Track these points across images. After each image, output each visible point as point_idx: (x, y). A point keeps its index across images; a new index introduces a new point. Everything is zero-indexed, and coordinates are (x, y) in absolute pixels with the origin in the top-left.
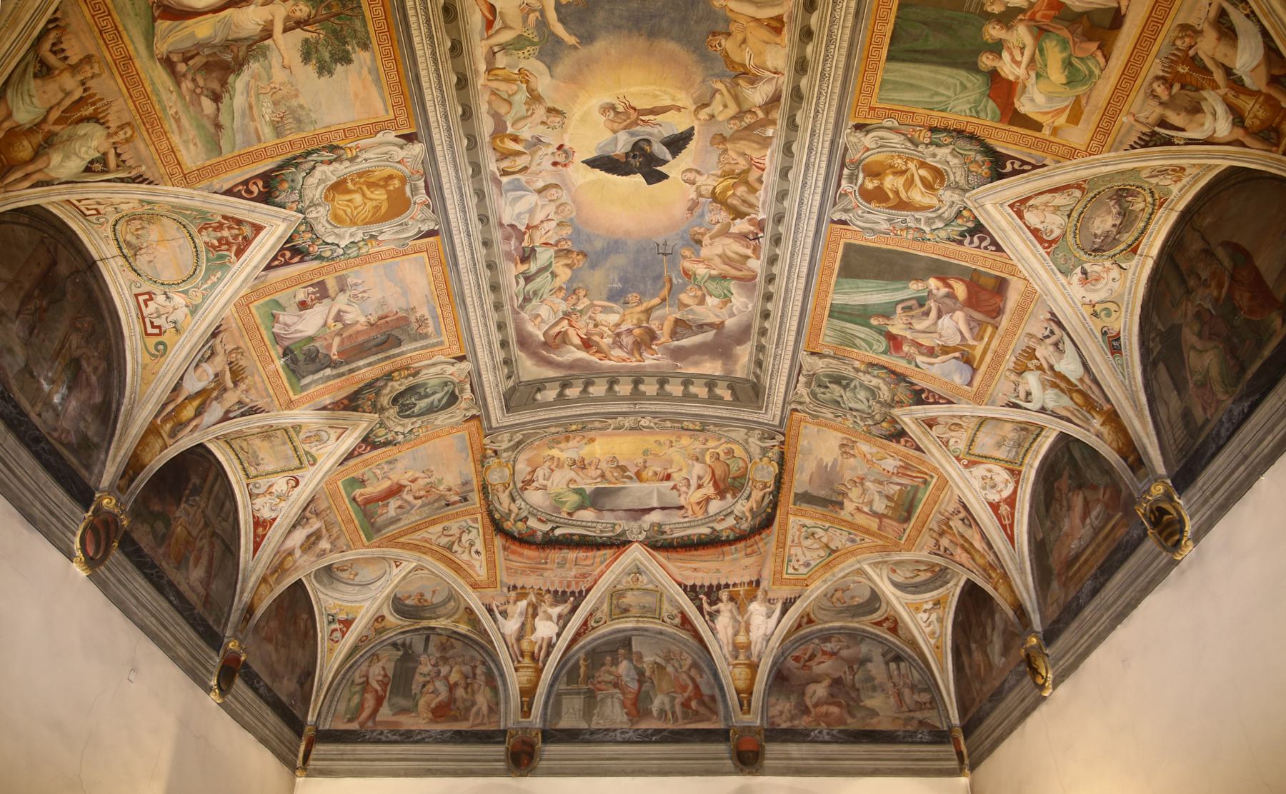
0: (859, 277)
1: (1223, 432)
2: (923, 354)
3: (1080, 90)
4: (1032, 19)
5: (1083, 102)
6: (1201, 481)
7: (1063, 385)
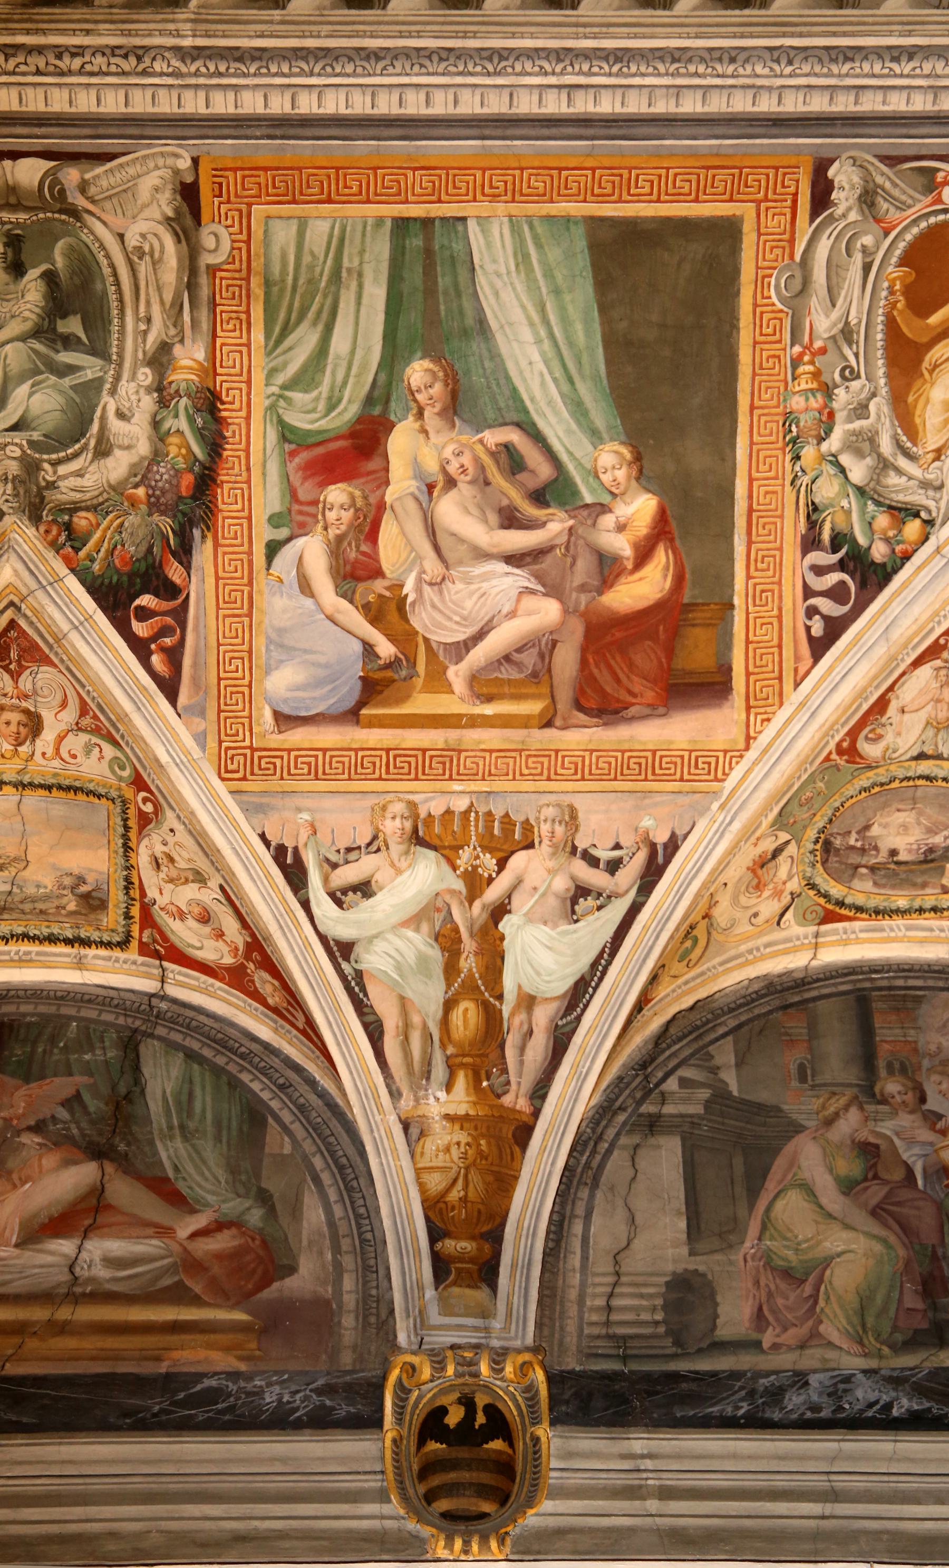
0: (603, 284)
1: (794, 1401)
2: (336, 549)
7: (469, 963)
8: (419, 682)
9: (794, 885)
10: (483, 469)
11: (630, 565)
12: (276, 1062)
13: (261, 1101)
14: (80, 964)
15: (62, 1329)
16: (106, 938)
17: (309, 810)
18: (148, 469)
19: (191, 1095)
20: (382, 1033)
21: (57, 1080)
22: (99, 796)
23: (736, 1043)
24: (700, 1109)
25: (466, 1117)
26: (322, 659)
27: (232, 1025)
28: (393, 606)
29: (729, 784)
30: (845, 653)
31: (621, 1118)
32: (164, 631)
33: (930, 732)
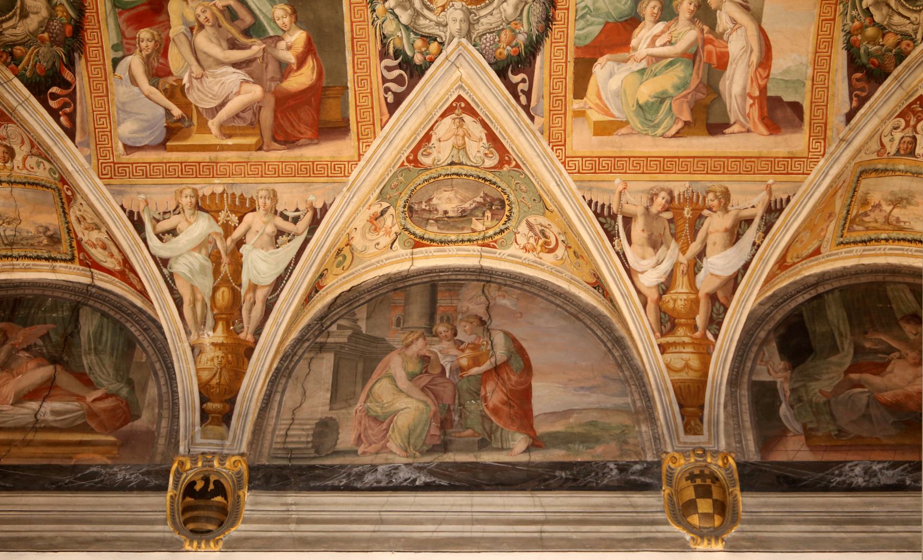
2: (147, 61)
3: (636, 123)
4: (705, 42)
5: (624, 131)
6: (291, 498)
8: (194, 128)
9: (396, 229)
10: (217, 19)
11: (295, 67)
12: (144, 318)
13: (134, 336)
14: (53, 270)
15: (28, 443)
16: (63, 257)
17: (144, 193)
18: (48, 23)
19: (101, 334)
20: (182, 303)
21: (39, 326)
22: (48, 188)
23: (368, 307)
24: (345, 340)
25: (222, 344)
26: (145, 118)
27: (125, 299)
28: (178, 90)
29: (351, 178)
30: (405, 111)
31: (307, 344)
32: (65, 105)
33: (455, 151)
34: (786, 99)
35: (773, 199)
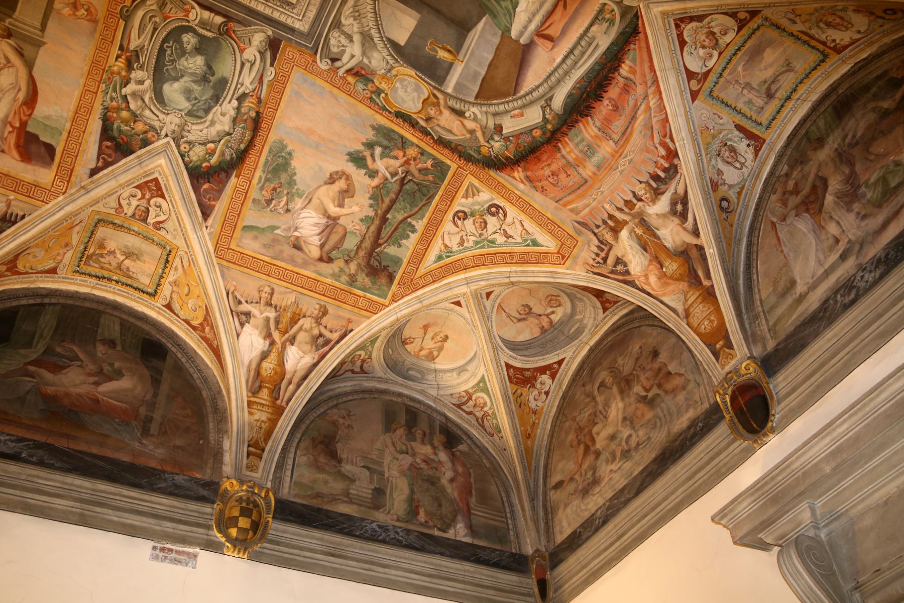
34: (44, 138)
35: (10, 211)
